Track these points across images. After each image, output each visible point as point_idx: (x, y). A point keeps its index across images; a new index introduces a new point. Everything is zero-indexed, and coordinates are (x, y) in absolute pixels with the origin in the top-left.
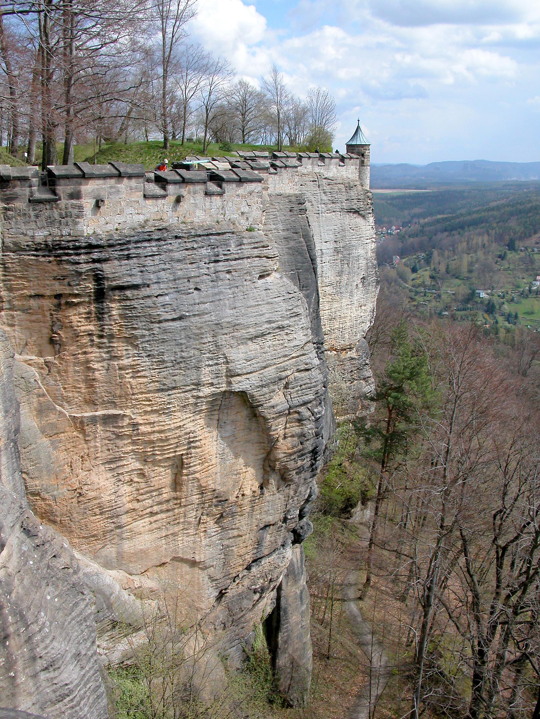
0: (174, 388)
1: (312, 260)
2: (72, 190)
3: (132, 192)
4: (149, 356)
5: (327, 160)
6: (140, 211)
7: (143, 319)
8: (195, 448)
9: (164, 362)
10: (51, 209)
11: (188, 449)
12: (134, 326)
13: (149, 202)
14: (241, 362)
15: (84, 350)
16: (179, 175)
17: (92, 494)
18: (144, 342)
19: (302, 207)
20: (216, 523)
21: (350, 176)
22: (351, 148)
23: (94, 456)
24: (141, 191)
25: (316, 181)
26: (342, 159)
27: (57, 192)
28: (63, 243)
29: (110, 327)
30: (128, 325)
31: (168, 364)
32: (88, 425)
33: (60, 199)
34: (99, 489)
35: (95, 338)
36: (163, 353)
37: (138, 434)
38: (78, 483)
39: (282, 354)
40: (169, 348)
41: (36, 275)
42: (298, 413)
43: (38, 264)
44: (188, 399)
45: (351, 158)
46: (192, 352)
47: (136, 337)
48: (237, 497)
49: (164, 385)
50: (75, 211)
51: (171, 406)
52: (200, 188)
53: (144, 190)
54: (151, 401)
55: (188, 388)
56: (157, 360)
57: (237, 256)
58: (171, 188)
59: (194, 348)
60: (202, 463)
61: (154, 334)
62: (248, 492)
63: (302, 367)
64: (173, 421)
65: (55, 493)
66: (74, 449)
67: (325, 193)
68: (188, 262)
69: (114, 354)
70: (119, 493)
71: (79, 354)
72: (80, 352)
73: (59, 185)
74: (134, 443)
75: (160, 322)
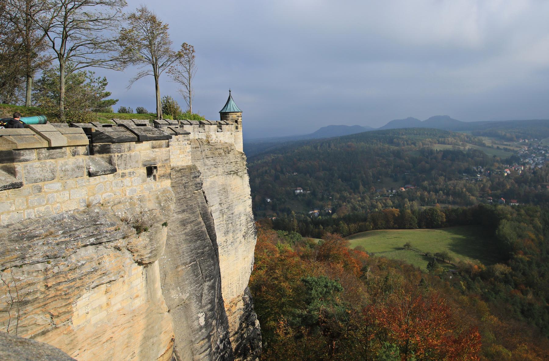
1: (212, 241)
19: (198, 180)
25: (198, 148)
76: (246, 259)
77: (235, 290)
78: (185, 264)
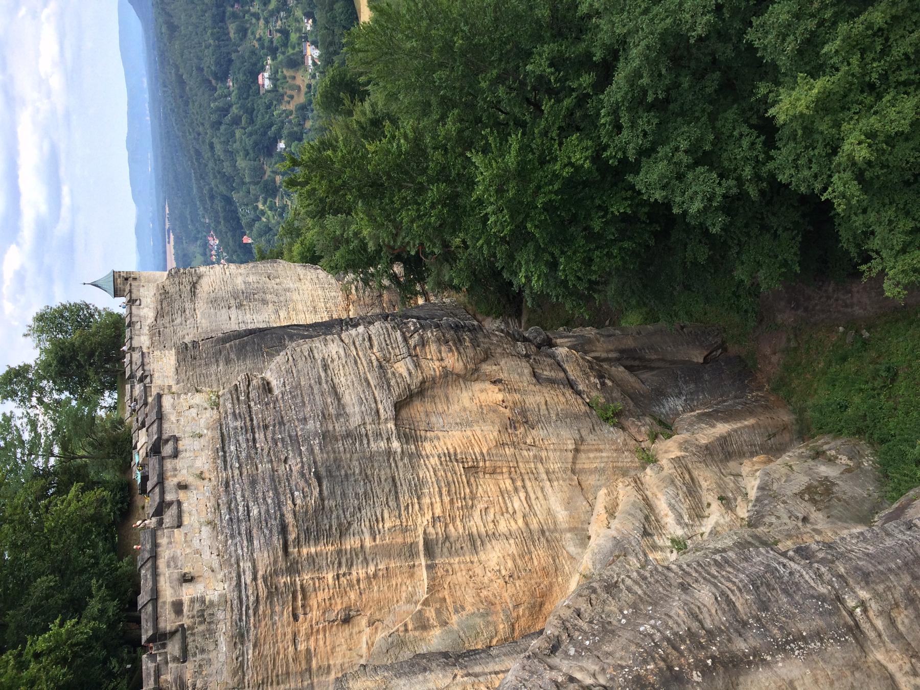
4: (359, 509)
5: (134, 319)
6: (197, 531)
7: (320, 518)
8: (455, 454)
9: (365, 493)
11: (457, 461)
12: (327, 527)
13: (186, 520)
14: (363, 408)
15: (355, 582)
16: (153, 488)
17: (510, 564)
19: (190, 345)
21: (153, 294)
22: (117, 293)
23: (470, 564)
26: (132, 302)
27: (174, 629)
33: (183, 625)
35: (341, 572)
37: (445, 517)
38: (499, 581)
40: (351, 488)
42: (415, 347)
44: (405, 465)
45: (130, 292)
47: (340, 525)
48: (506, 407)
49: (390, 491)
50: (197, 606)
52: (169, 464)
53: (172, 527)
54: (408, 505)
55: (393, 465)
57: (248, 419)
58: (169, 497)
62: (500, 397)
63: (367, 344)
65: (511, 606)
67: (173, 321)
70: (508, 534)
74: (453, 520)
76: (302, 277)
77: (333, 294)
78: (264, 362)
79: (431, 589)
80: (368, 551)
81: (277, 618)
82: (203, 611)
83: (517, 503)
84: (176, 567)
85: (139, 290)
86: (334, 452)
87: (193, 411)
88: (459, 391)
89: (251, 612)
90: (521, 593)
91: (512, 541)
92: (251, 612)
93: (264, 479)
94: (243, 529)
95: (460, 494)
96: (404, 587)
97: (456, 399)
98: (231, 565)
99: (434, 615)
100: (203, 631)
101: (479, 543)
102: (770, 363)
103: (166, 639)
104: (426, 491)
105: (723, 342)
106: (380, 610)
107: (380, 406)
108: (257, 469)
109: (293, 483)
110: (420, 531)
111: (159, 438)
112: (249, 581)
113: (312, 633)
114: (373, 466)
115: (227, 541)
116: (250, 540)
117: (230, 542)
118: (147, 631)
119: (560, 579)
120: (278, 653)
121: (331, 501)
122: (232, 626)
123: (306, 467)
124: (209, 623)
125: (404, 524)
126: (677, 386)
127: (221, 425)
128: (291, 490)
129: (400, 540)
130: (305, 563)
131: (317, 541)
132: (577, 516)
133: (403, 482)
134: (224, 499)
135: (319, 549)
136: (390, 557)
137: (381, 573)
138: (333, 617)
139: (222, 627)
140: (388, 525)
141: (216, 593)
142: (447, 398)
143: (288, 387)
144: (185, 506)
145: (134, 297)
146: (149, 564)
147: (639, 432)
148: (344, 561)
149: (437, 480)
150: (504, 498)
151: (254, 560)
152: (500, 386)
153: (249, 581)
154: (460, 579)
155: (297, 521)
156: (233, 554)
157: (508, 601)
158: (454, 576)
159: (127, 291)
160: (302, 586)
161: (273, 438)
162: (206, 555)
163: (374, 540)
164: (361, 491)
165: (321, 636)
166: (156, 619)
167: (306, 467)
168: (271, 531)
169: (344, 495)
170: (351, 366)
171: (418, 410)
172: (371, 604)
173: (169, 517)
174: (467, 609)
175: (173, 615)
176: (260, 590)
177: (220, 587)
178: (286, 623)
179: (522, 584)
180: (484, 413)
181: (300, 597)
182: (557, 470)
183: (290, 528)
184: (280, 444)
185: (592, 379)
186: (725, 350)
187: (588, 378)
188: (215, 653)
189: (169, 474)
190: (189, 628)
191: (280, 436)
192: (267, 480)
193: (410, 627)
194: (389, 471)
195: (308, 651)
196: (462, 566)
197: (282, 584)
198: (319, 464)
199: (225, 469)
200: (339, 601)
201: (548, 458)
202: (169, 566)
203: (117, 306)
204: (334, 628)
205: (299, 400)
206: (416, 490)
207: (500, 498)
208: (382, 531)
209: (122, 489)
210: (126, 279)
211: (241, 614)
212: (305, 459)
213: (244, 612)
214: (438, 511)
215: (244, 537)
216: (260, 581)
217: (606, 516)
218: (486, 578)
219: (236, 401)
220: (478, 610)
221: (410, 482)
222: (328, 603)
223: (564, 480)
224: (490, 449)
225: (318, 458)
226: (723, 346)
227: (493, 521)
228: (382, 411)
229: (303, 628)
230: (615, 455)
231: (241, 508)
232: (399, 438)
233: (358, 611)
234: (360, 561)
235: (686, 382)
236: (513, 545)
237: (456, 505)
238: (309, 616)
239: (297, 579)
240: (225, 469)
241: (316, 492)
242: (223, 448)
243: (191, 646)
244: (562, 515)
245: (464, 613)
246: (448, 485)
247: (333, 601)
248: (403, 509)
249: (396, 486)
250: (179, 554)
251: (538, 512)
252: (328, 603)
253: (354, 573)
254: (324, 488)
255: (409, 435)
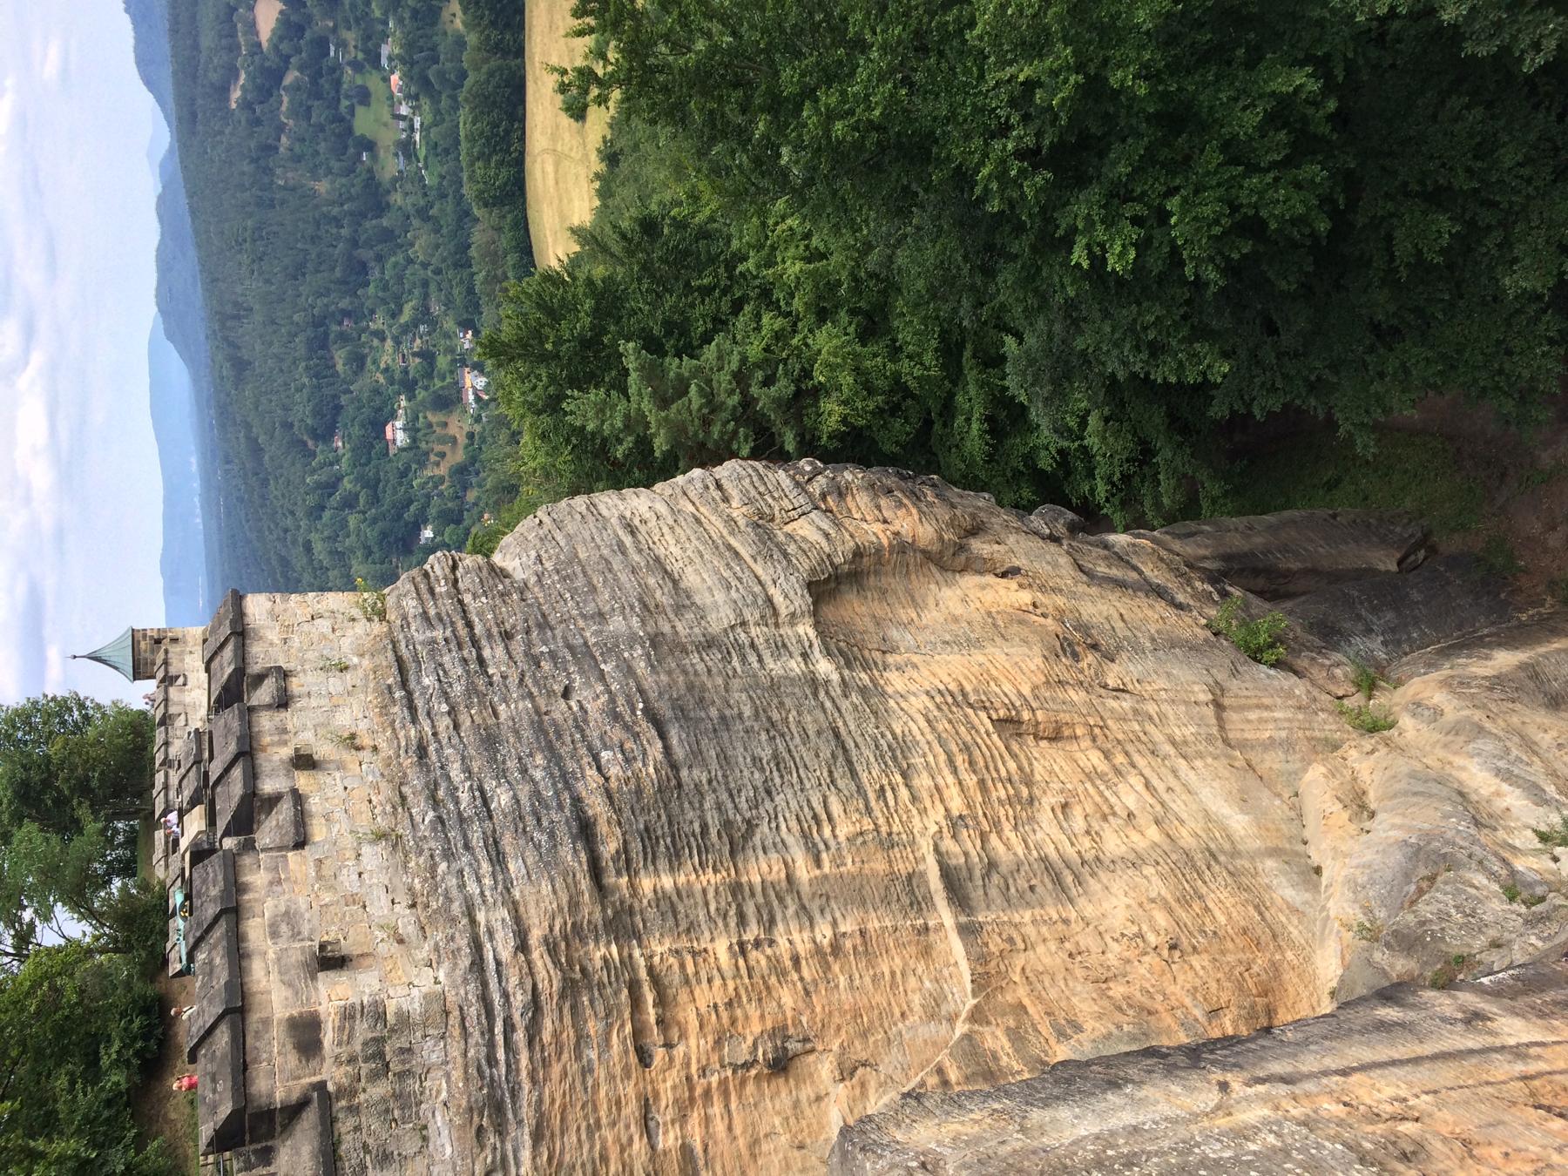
0: (837, 735)
2: (289, 1047)
3: (288, 879)
4: (769, 792)
5: (172, 710)
6: (350, 854)
7: (674, 805)
8: (964, 695)
9: (776, 756)
10: (354, 1110)
11: (970, 705)
12: (698, 830)
13: (318, 831)
14: (734, 594)
15: (788, 964)
16: (227, 770)
17: (1162, 919)
18: (736, 807)
20: (1113, 661)
22: (140, 671)
23: (1060, 926)
24: (285, 857)
27: (295, 1096)
28: (471, 1053)
29: (711, 895)
30: (698, 846)
31: (781, 748)
32: (986, 944)
34: (1141, 905)
35: (749, 936)
36: (754, 759)
37: (975, 818)
38: (1146, 959)
39: (696, 526)
40: (739, 745)
41: (584, 1137)
42: (824, 496)
43: (548, 1134)
44: (856, 708)
45: (166, 663)
46: (736, 695)
47: (727, 824)
48: (1044, 615)
49: (833, 755)
50: (363, 1030)
51: (882, 741)
52: (266, 722)
53: (280, 849)
54: (882, 788)
55: (828, 704)
56: (776, 774)
57: (460, 624)
58: (268, 786)
59: (727, 691)
60: (995, 680)
61: (710, 782)
62: (1025, 597)
63: (717, 495)
64: (919, 737)
65: (1198, 1013)
66: (1059, 977)
68: (491, 721)
69: (784, 884)
70: (1132, 856)
71: (802, 979)
72: (795, 977)
73: (271, 1095)
74: (996, 825)
75: (674, 767)
79: (981, 983)
80: (805, 889)
81: (593, 1055)
82: (379, 1041)
83: (1129, 795)
84: (296, 935)
85: (182, 660)
86: (685, 672)
87: (324, 625)
88: (933, 586)
89: (520, 1036)
90: (1213, 986)
91: (1149, 870)
92: (520, 1036)
93: (516, 732)
94: (476, 838)
95: (997, 770)
96: (912, 982)
97: (931, 602)
98: (453, 921)
99: (1007, 1045)
100: (383, 1100)
101: (1069, 879)
102: (1545, 551)
103: (271, 1135)
104: (917, 761)
105: (1427, 535)
106: (864, 1035)
107: (772, 591)
108: (496, 714)
109: (594, 735)
110: (925, 847)
111: (240, 671)
112: (506, 955)
113: (692, 1099)
114: (782, 704)
115: (433, 868)
116: (498, 859)
117: (443, 866)
118: (214, 1109)
119: (1290, 955)
120: (604, 1158)
121: (696, 772)
122: (467, 1080)
123: (621, 700)
124: (401, 1076)
125: (884, 829)
126: (1359, 617)
127: (394, 644)
128: (590, 748)
129: (880, 866)
130: (651, 913)
131: (675, 860)
132: (1270, 826)
133: (859, 740)
134: (416, 780)
135: (682, 879)
136: (864, 903)
137: (848, 944)
138: (743, 1055)
139: (438, 1087)
140: (844, 830)
141: (415, 992)
142: (913, 598)
143: (549, 565)
144: (314, 804)
145: (173, 671)
146: (219, 932)
147: (1332, 678)
148: (750, 909)
149: (939, 738)
150: (1094, 784)
151: (515, 904)
152: (1019, 578)
153: (506, 955)
154: (1047, 960)
155: (618, 812)
156: (454, 893)
157: (1188, 1001)
158: (1030, 953)
159: (159, 661)
160: (651, 970)
161: (526, 654)
162: (379, 906)
163: (818, 863)
164: (766, 754)
165: (717, 1109)
166: (241, 1067)
167: (621, 700)
168: (552, 835)
169: (725, 759)
170: (686, 529)
171: (855, 610)
172: (837, 1020)
173: (269, 831)
174: (1088, 1026)
175: (293, 1059)
176: (541, 974)
177: (425, 981)
178: (618, 1070)
179: (1206, 963)
180: (997, 627)
181: (649, 997)
182: (1191, 739)
183: (602, 828)
184: (546, 665)
185: (1198, 584)
186: (1433, 550)
187: (1189, 582)
188: (420, 1164)
189: (267, 740)
190: (342, 1092)
191: (544, 649)
192: (527, 734)
193: (953, 1075)
194: (822, 717)
195: (686, 1150)
196: (1044, 929)
197: (599, 963)
198: (653, 695)
199: (414, 720)
200: (753, 1010)
201: (1162, 716)
202: (275, 934)
203: (138, 695)
204: (750, 1088)
205: (580, 582)
206: (894, 758)
207: (1088, 785)
208: (832, 843)
209: (145, 1010)
210: (158, 642)
211: (491, 1045)
212: (615, 687)
213: (500, 1039)
214: (957, 805)
215: (481, 854)
216: (538, 954)
217: (1346, 815)
218: (1109, 955)
219: (426, 596)
220: (1119, 1027)
221: (875, 740)
222: (725, 1015)
223: (1215, 758)
224: (1035, 688)
225: (649, 682)
226: (1424, 541)
227: (1088, 832)
228: (778, 599)
229: (668, 1088)
230: (1301, 717)
231: (464, 797)
232: (828, 653)
233: (806, 1040)
234: (791, 911)
235: (1375, 610)
236: (1155, 880)
237: (994, 795)
238: (679, 1051)
239: (637, 953)
240: (414, 720)
241: (656, 750)
242: (404, 684)
243: (348, 1144)
244: (1239, 823)
245: (1081, 1036)
246: (966, 748)
247: (739, 1012)
248: (872, 796)
249: (845, 750)
250: (303, 906)
251: (1184, 816)
252: (725, 1015)
253: (782, 942)
254: (674, 741)
255: (848, 653)
